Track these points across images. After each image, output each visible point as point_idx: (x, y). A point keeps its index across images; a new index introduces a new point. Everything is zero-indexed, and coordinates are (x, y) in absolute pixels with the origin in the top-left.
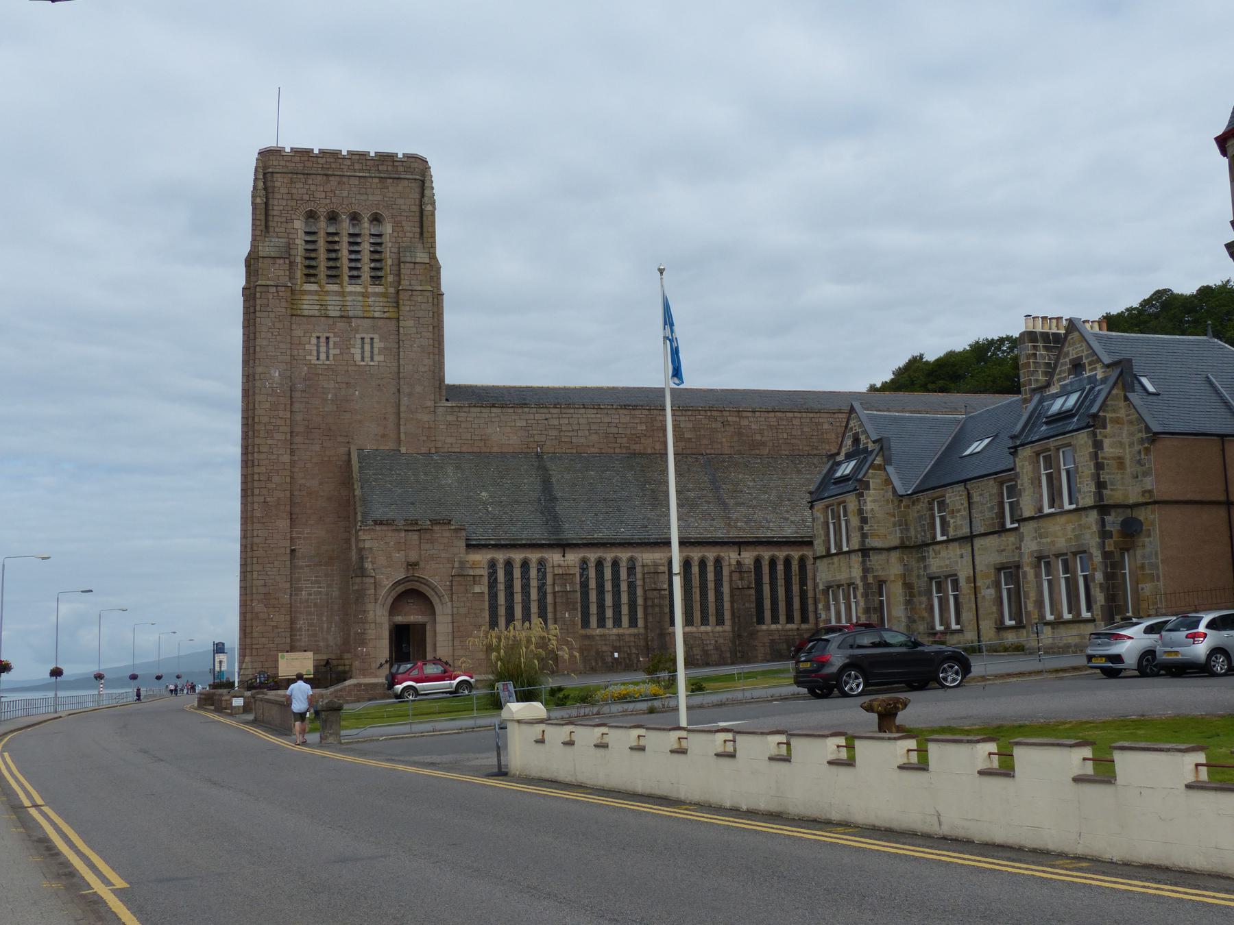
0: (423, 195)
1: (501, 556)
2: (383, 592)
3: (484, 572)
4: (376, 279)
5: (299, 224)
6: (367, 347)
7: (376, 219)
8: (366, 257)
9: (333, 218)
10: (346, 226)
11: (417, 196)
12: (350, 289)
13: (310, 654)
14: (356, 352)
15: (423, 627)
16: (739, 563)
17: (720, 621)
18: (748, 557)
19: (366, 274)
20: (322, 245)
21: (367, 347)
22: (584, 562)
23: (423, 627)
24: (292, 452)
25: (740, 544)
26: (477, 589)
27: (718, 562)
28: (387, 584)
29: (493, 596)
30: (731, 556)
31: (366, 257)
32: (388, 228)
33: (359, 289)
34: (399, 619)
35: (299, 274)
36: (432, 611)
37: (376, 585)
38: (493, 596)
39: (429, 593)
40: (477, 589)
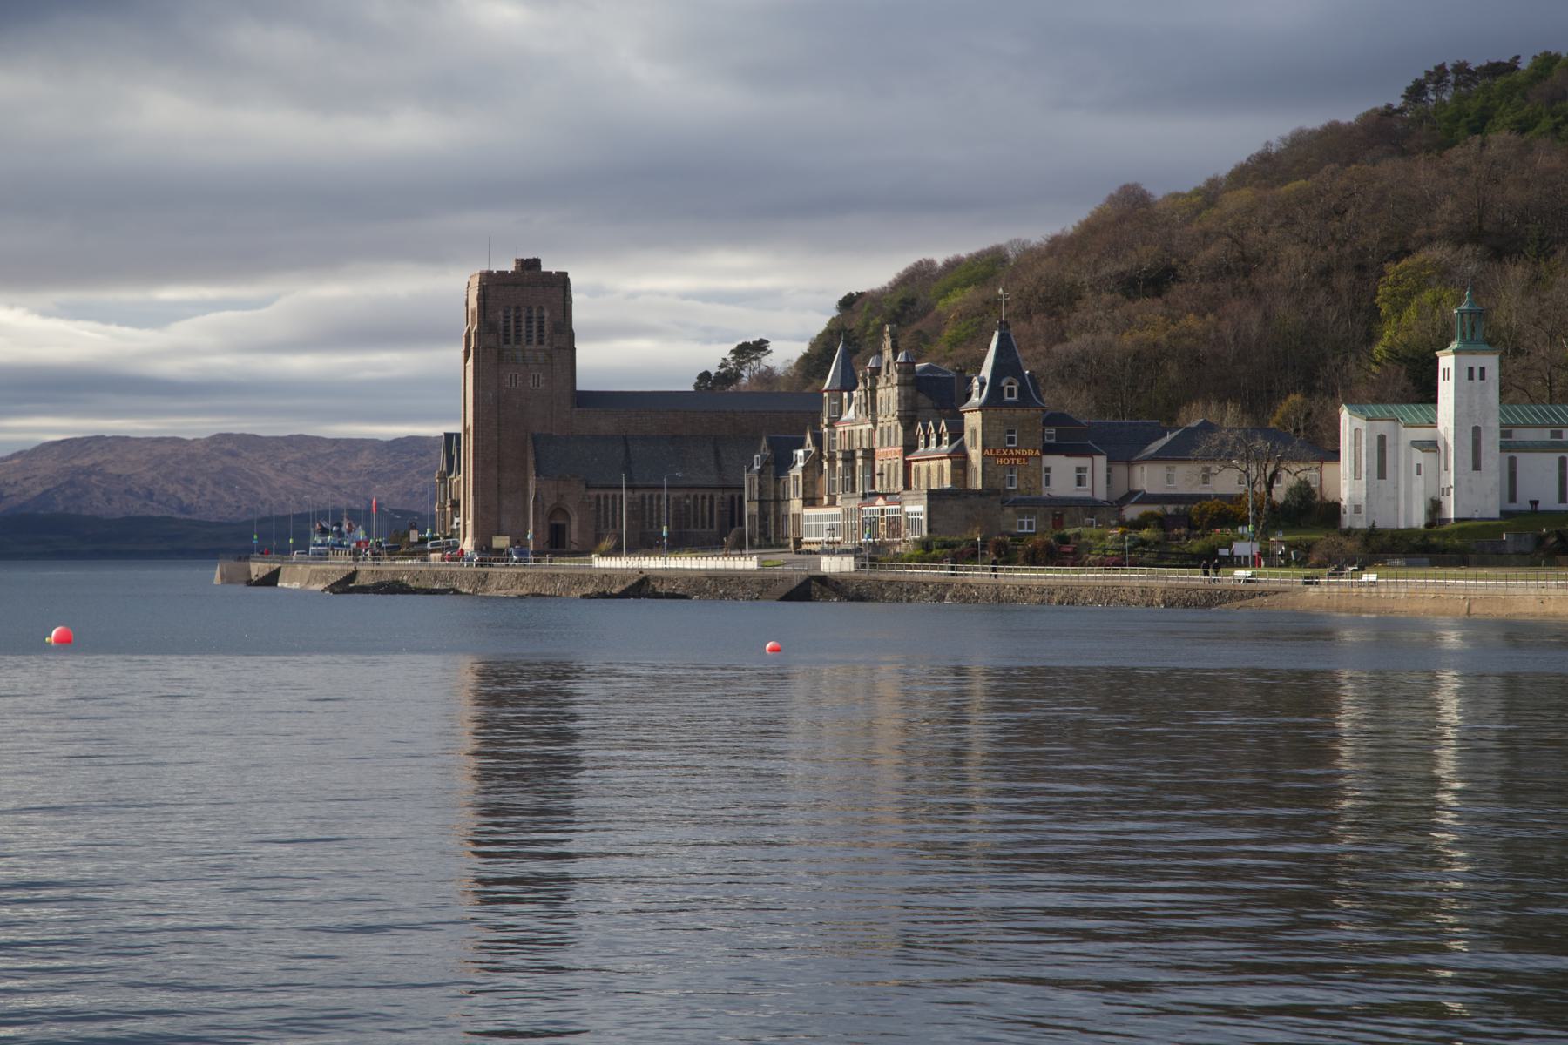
0: (565, 295)
1: (602, 493)
2: (546, 509)
3: (593, 500)
4: (541, 342)
5: (501, 313)
6: (536, 380)
7: (541, 309)
8: (535, 329)
9: (518, 309)
10: (524, 313)
11: (562, 295)
12: (527, 347)
13: (508, 538)
14: (531, 381)
15: (564, 526)
16: (722, 498)
17: (711, 526)
18: (727, 494)
19: (535, 340)
20: (512, 323)
21: (536, 380)
22: (643, 498)
23: (564, 526)
24: (499, 435)
25: (723, 488)
26: (591, 509)
27: (712, 498)
28: (548, 505)
29: (598, 510)
30: (718, 495)
31: (535, 329)
32: (546, 314)
33: (532, 347)
34: (553, 522)
35: (501, 340)
36: (568, 518)
37: (543, 505)
38: (598, 510)
39: (567, 509)
40: (591, 509)
